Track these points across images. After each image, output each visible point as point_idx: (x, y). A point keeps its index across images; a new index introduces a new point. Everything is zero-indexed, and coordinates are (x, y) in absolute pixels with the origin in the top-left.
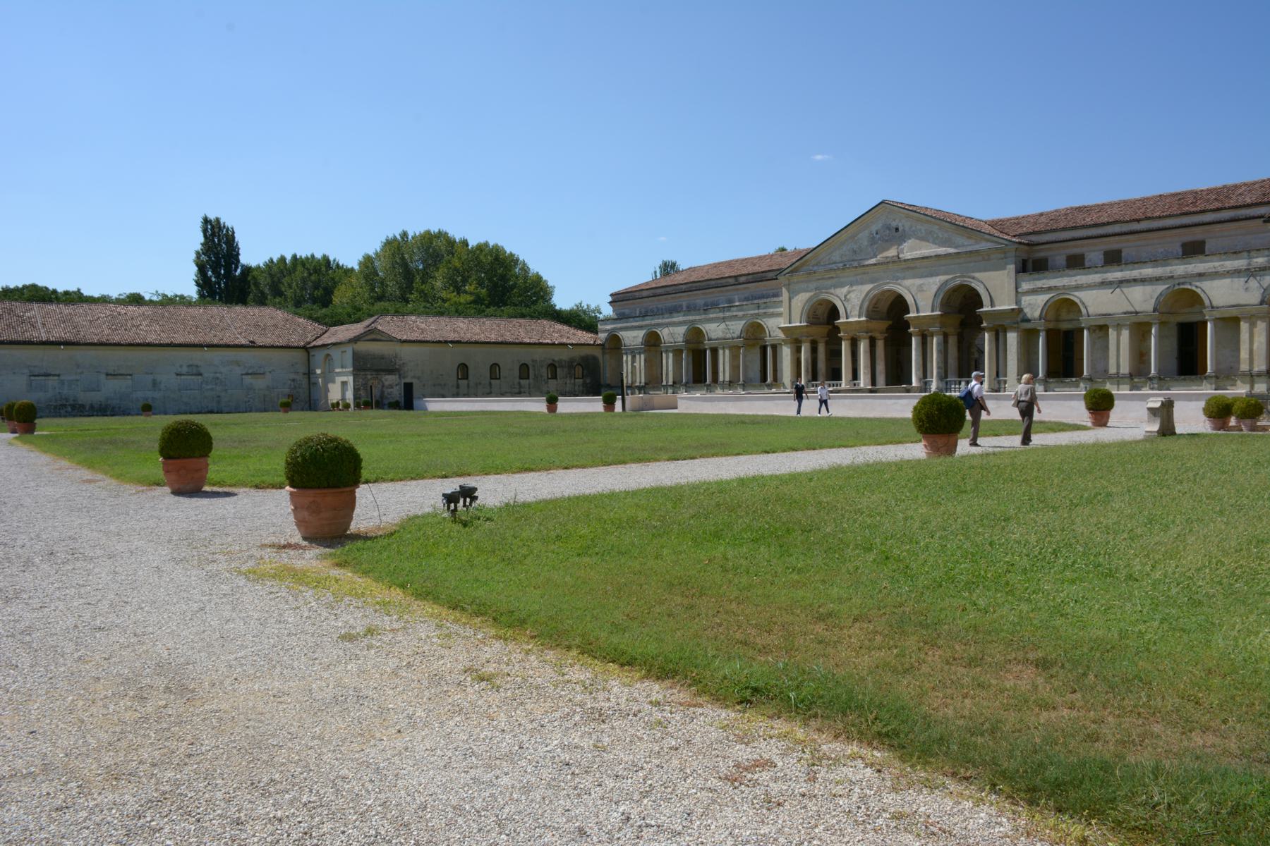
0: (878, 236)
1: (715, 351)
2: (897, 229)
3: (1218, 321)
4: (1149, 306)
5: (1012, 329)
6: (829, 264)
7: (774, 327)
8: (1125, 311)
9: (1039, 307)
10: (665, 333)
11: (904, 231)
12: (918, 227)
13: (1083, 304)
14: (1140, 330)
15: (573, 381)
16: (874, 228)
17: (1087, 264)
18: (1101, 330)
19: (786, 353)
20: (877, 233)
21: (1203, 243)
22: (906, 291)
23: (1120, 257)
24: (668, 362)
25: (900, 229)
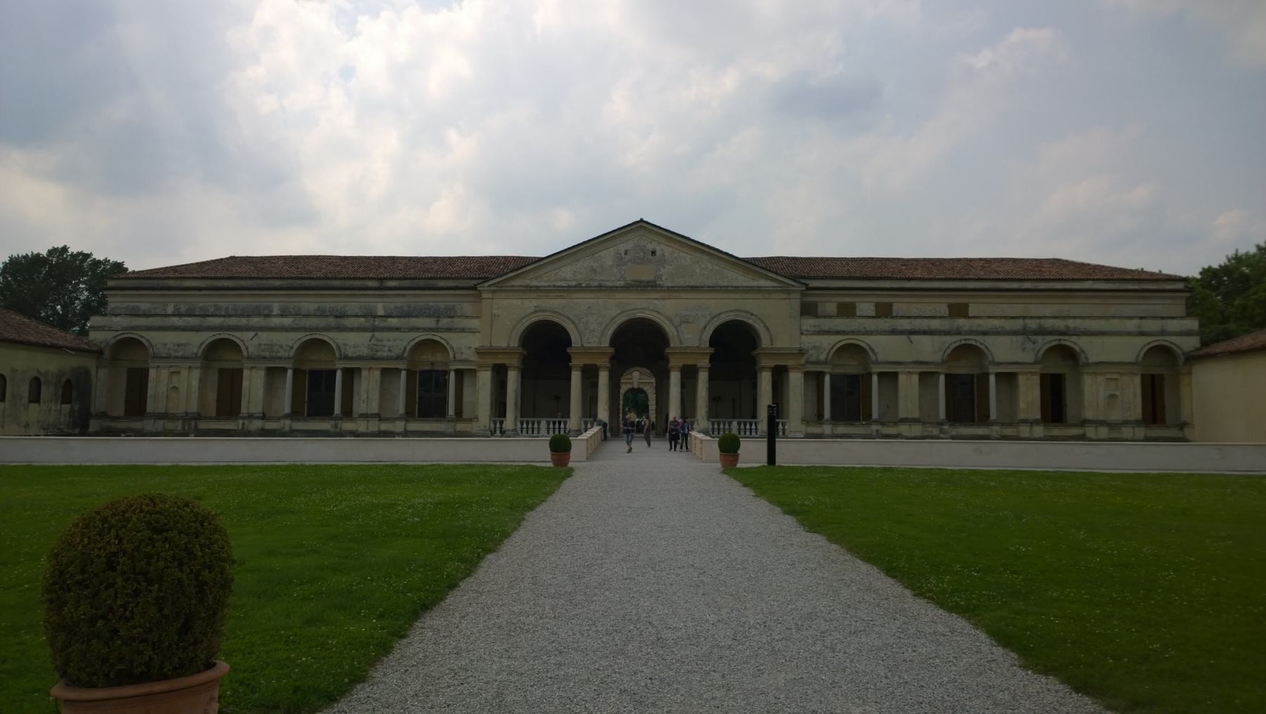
0: (627, 257)
1: (350, 374)
2: (653, 253)
3: (998, 375)
4: (937, 358)
5: (796, 368)
6: (556, 280)
7: (463, 346)
8: (915, 360)
9: (825, 350)
10: (249, 341)
11: (663, 255)
12: (682, 254)
13: (873, 350)
14: (926, 377)
15: (58, 407)
16: (622, 248)
17: (858, 313)
18: (890, 378)
19: (485, 377)
20: (626, 254)
21: (966, 306)
22: (667, 322)
23: (891, 310)
24: (253, 384)
25: (658, 253)
